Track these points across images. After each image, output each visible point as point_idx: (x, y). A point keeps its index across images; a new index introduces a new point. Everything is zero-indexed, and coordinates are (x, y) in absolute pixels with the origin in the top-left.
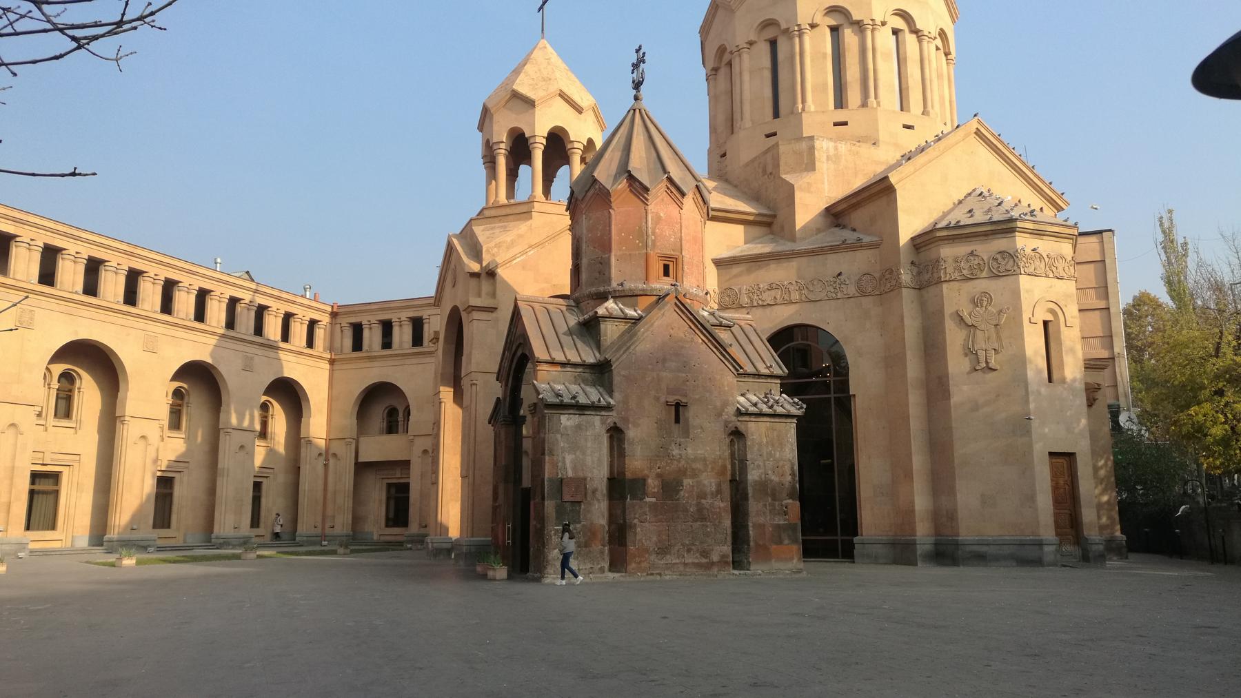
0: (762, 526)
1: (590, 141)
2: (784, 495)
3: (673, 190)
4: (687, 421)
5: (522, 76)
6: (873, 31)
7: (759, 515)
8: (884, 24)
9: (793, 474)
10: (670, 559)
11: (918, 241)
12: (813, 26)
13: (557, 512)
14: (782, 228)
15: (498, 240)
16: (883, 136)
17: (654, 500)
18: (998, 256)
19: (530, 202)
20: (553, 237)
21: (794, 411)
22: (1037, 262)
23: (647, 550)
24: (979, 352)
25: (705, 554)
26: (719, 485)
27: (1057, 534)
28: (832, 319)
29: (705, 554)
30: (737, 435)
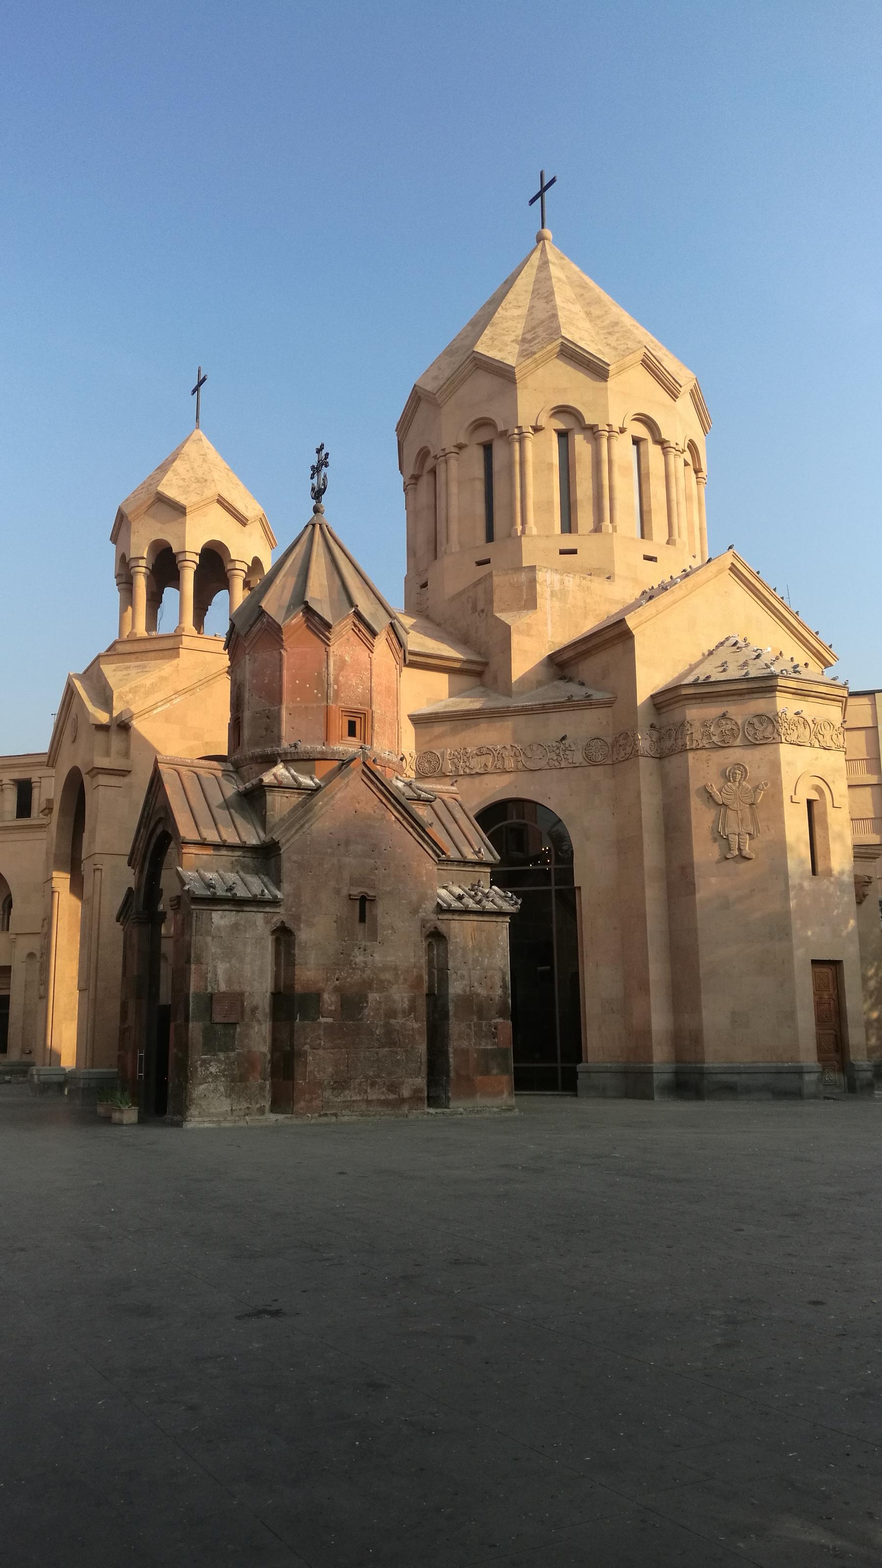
0: (464, 1052)
1: (256, 562)
2: (493, 1013)
3: (362, 627)
4: (374, 919)
5: (170, 475)
6: (609, 439)
7: (461, 1036)
8: (622, 430)
9: (504, 987)
10: (349, 1095)
12: (537, 429)
13: (204, 1037)
14: (495, 679)
15: (133, 684)
16: (619, 569)
17: (330, 1020)
18: (755, 720)
19: (178, 635)
20: (207, 682)
21: (506, 907)
22: (801, 728)
23: (320, 1084)
25: (393, 1088)
26: (413, 1001)
27: (820, 1060)
28: (554, 793)
29: (393, 1088)
30: (436, 937)
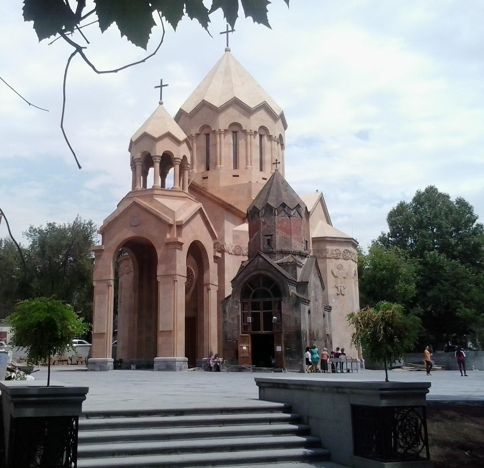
11: (315, 240)
24: (338, 287)
